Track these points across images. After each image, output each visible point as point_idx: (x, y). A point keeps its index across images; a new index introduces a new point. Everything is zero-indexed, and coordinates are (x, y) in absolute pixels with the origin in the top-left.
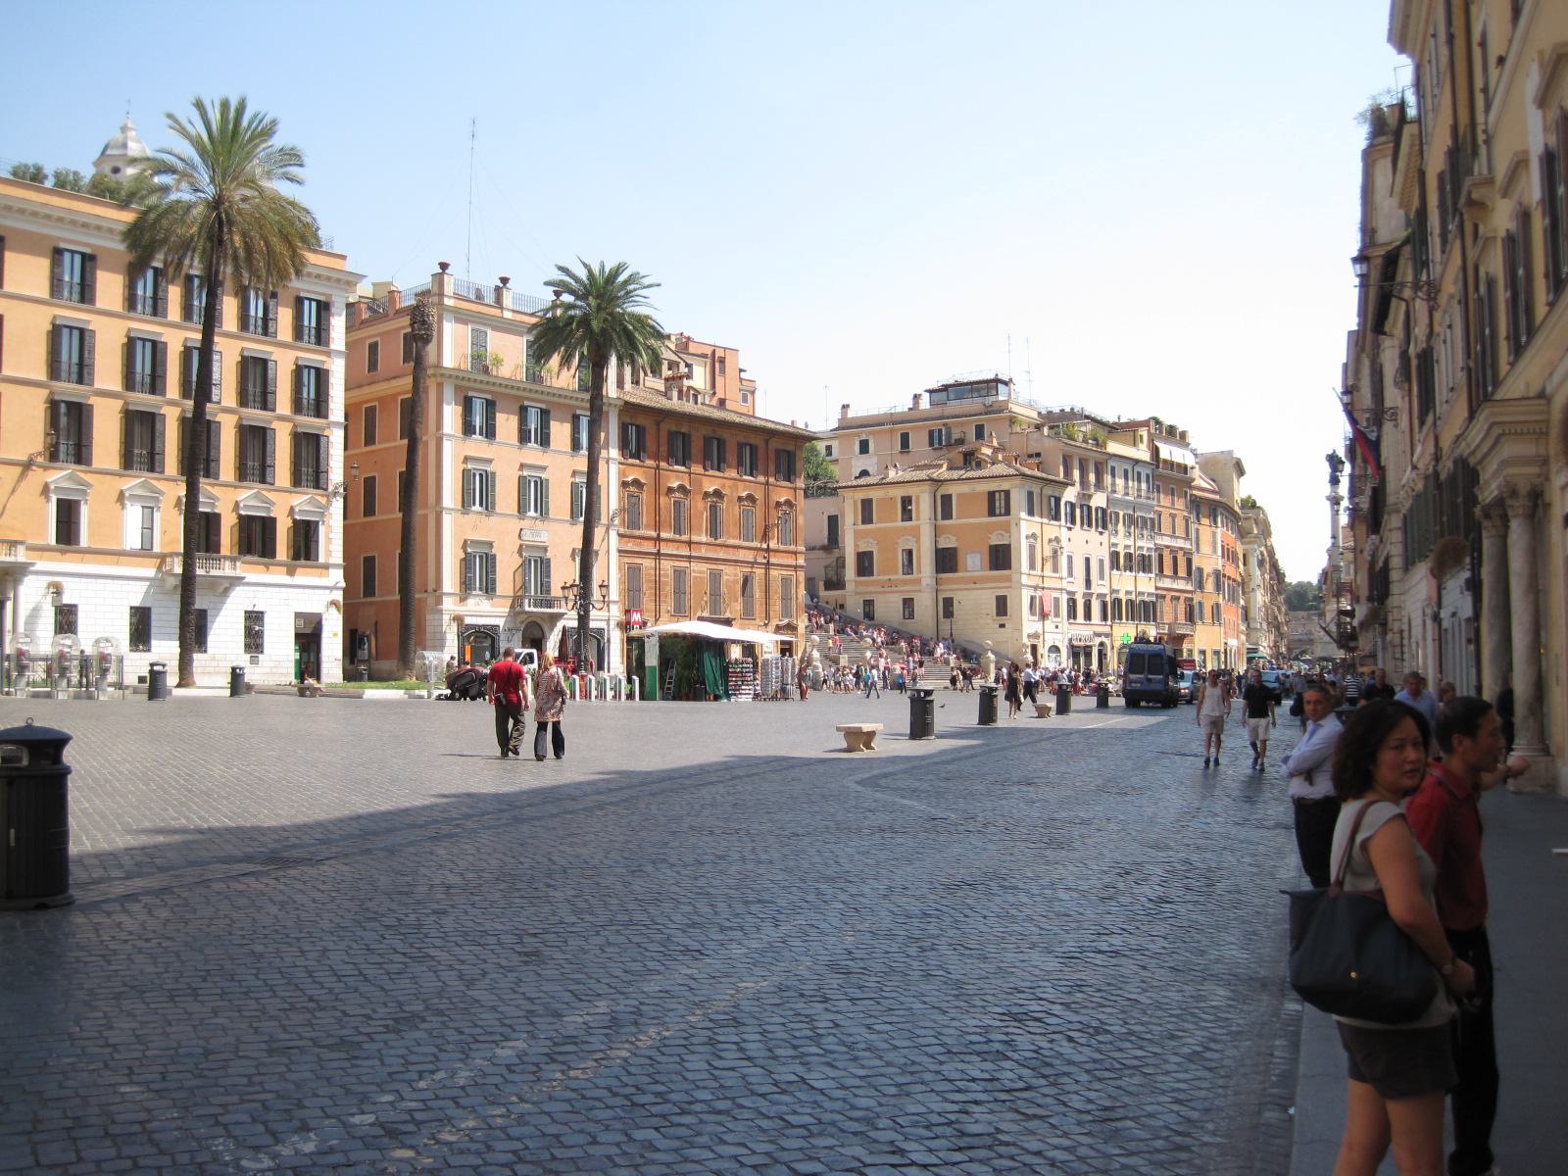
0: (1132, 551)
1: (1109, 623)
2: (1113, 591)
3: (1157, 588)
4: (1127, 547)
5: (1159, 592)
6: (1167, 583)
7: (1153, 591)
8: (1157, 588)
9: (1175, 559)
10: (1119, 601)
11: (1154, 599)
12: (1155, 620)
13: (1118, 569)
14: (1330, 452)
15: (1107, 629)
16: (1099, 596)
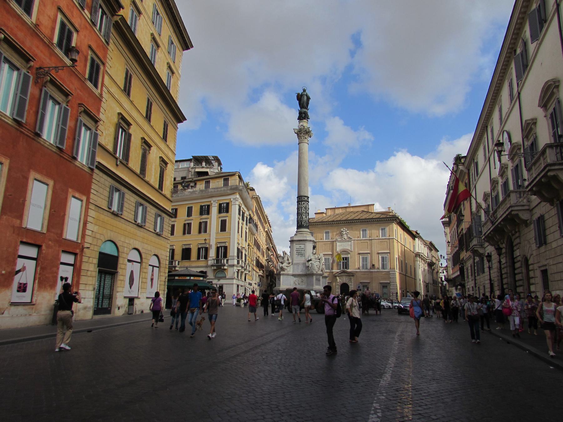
14: (300, 92)
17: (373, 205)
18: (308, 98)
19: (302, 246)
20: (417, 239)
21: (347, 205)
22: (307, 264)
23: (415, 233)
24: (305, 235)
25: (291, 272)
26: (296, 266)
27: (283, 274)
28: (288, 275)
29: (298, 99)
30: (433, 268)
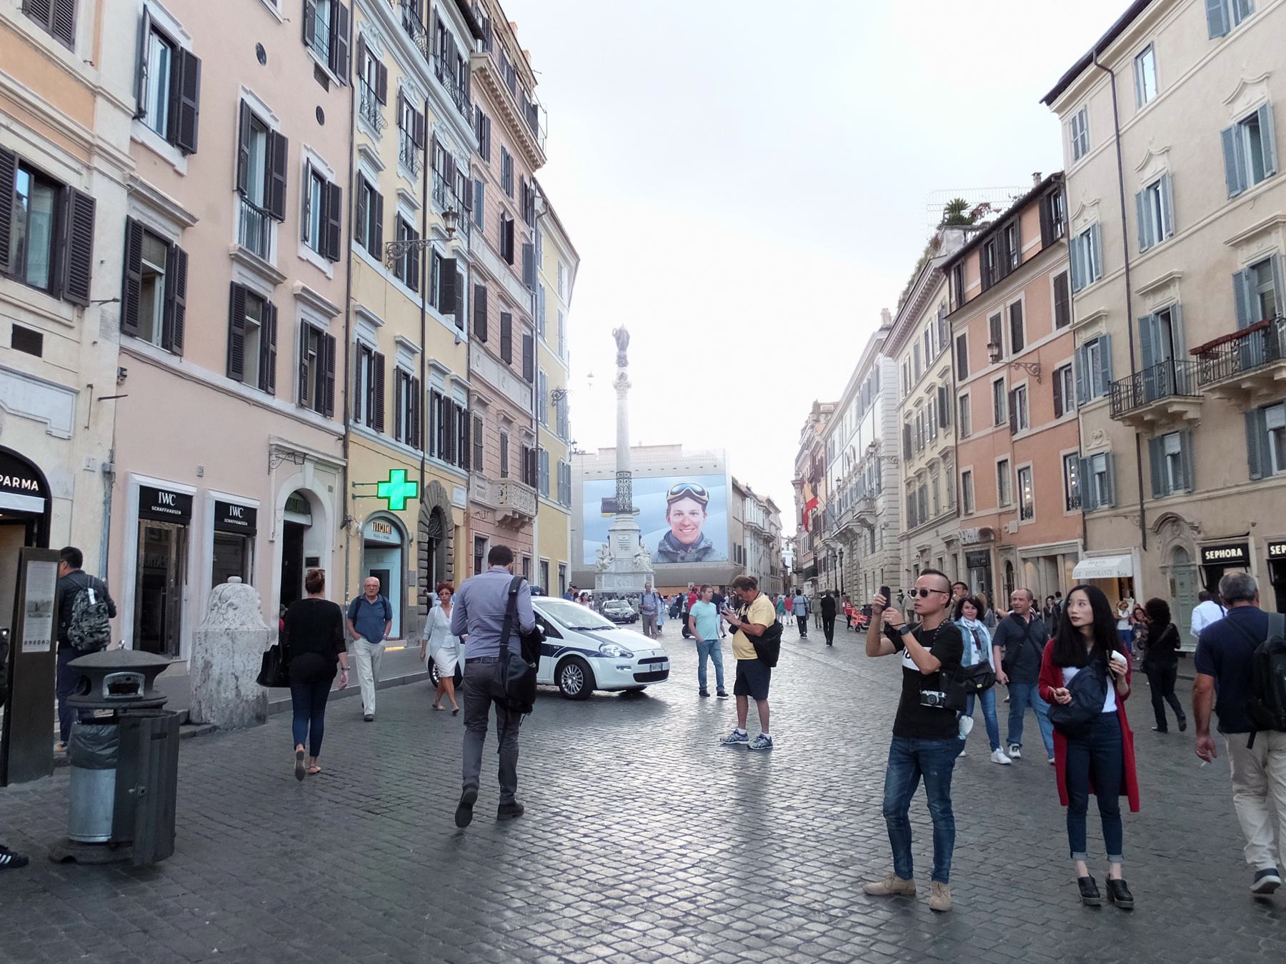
0: (416, 225)
1: (336, 425)
2: (353, 313)
3: (470, 373)
4: (402, 196)
5: (474, 385)
6: (489, 371)
7: (463, 377)
8: (470, 373)
9: (506, 320)
10: (378, 362)
11: (459, 398)
12: (465, 464)
13: (375, 251)
15: (331, 448)
16: (304, 297)
17: (681, 445)
18: (628, 337)
19: (627, 537)
20: (748, 500)
21: (638, 445)
22: (635, 561)
23: (744, 490)
24: (629, 523)
25: (613, 571)
26: (619, 563)
27: (605, 573)
28: (610, 573)
29: (614, 335)
30: (771, 544)
